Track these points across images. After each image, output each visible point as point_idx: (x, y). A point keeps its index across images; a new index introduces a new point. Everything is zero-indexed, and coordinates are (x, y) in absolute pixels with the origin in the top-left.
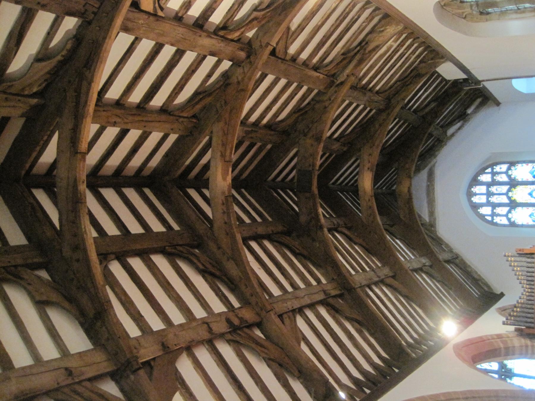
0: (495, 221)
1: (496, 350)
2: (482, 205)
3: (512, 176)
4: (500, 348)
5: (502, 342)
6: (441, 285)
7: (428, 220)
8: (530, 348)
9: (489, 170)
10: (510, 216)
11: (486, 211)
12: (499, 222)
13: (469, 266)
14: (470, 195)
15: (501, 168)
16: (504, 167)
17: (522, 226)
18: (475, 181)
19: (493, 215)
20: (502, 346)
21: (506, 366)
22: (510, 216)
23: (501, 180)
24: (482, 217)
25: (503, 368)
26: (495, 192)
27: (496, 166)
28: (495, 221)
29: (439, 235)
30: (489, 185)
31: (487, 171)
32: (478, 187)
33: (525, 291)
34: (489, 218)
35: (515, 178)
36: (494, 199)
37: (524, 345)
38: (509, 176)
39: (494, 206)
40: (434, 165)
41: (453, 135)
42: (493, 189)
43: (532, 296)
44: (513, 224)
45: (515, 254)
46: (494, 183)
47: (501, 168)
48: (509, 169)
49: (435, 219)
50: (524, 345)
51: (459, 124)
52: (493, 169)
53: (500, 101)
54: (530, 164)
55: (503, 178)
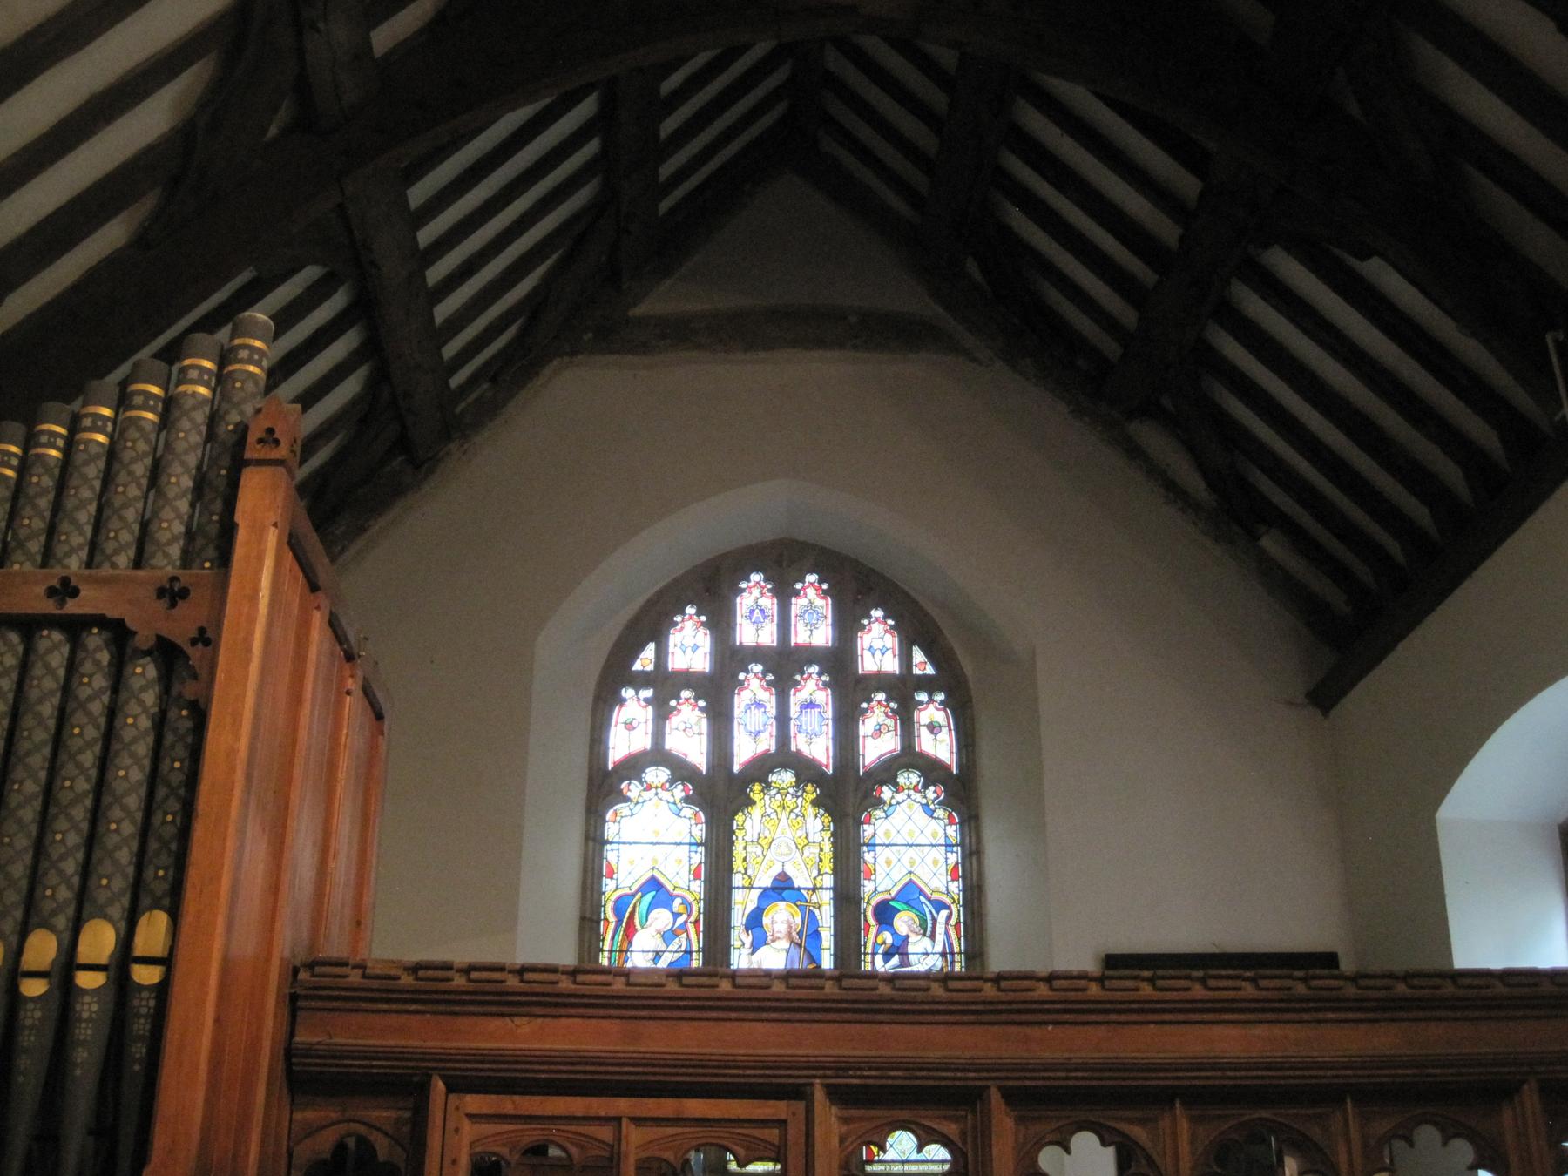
0: (627, 693)
2: (720, 622)
3: (886, 793)
7: (638, 311)
9: (922, 665)
10: (657, 775)
11: (689, 644)
12: (621, 715)
13: (362, 530)
14: (779, 563)
15: (933, 728)
16: (940, 746)
17: (594, 841)
18: (858, 588)
19: (665, 686)
22: (657, 775)
23: (866, 728)
24: (652, 624)
26: (796, 699)
27: (945, 704)
28: (627, 693)
29: (547, 371)
30: (838, 663)
31: (918, 656)
32: (824, 606)
34: (645, 660)
35: (879, 803)
36: (753, 697)
38: (887, 772)
39: (716, 693)
41: (1134, 451)
42: (813, 688)
44: (604, 787)
46: (851, 690)
47: (933, 728)
48: (931, 770)
49: (643, 348)
51: (1195, 483)
52: (927, 684)
53: (1333, 712)
54: (956, 887)
55: (877, 740)
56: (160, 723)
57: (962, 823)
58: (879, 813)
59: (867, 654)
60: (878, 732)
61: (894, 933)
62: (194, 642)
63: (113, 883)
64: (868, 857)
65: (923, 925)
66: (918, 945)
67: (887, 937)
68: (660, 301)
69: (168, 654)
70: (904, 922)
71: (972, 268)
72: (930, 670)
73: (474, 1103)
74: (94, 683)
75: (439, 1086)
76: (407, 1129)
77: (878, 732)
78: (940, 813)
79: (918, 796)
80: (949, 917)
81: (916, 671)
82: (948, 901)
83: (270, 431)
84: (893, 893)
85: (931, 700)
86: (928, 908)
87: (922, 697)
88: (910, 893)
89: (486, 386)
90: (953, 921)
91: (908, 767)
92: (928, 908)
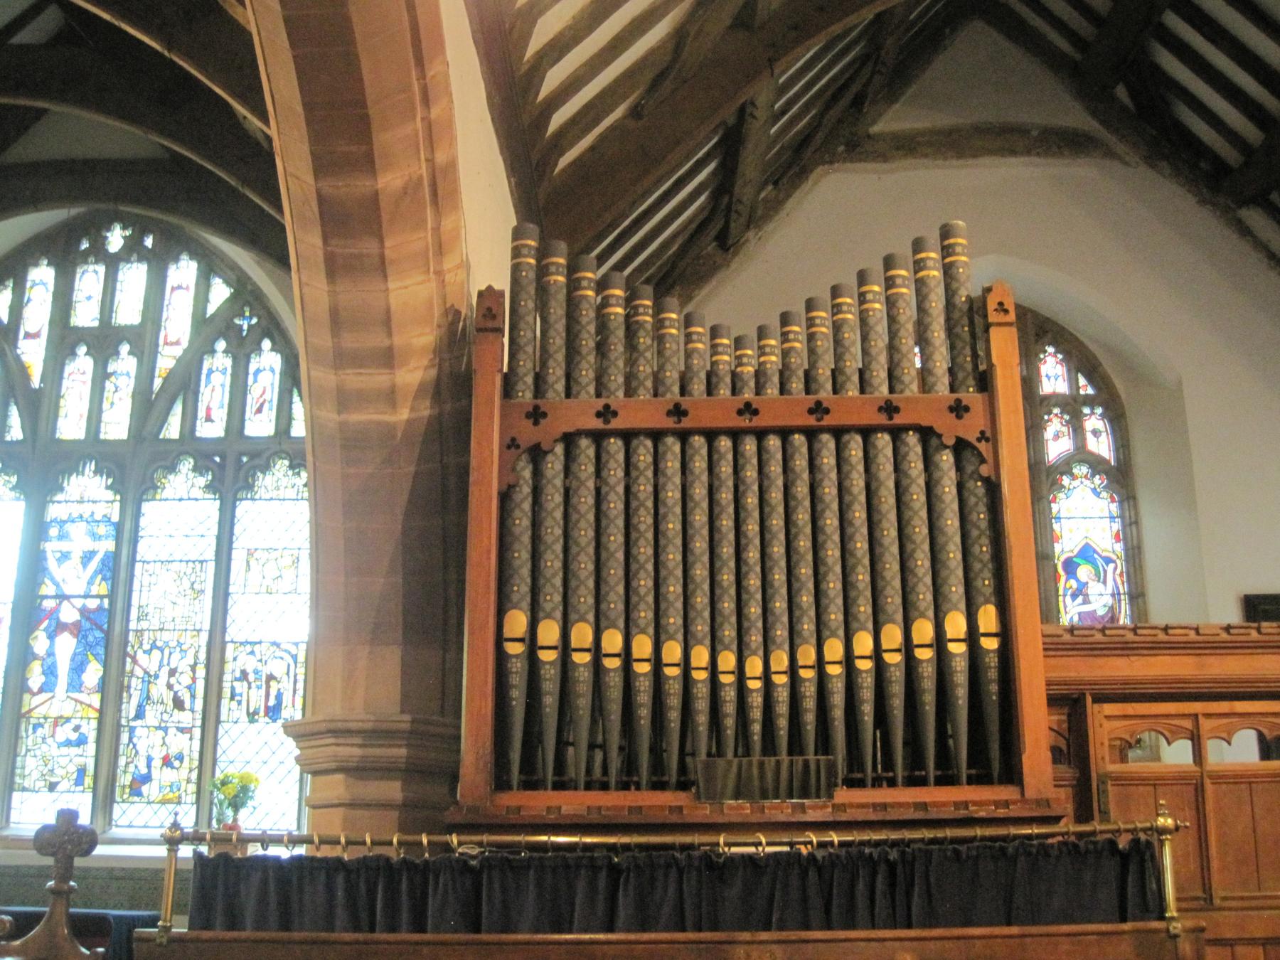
1: (361, 127)
3: (1066, 480)
4: (367, 163)
5: (410, 190)
6: (652, 52)
7: (875, 129)
8: (377, 379)
15: (1096, 433)
16: (1102, 446)
20: (389, 181)
21: (266, 468)
23: (1049, 433)
25: (253, 456)
27: (1103, 416)
29: (813, 176)
31: (1082, 381)
33: (739, 343)
37: (398, 340)
38: (1065, 466)
40: (1110, 154)
41: (1245, 231)
43: (710, 391)
45: (968, 289)
47: (1096, 433)
48: (1097, 465)
50: (398, 340)
52: (1090, 401)
54: (1119, 547)
56: (960, 487)
57: (1121, 502)
58: (1061, 495)
59: (1044, 379)
60: (1057, 437)
61: (1078, 580)
62: (979, 440)
63: (956, 590)
64: (1056, 526)
65: (1097, 575)
66: (1094, 588)
67: (1073, 583)
68: (892, 120)
69: (960, 447)
70: (1084, 572)
71: (1121, 92)
72: (1090, 391)
73: (1109, 709)
74: (915, 466)
75: (1089, 699)
76: (1065, 726)
77: (1057, 437)
78: (1104, 494)
79: (1087, 482)
80: (1115, 569)
81: (1082, 392)
82: (1114, 557)
83: (1001, 304)
84: (1076, 552)
85: (1093, 413)
86: (1100, 562)
87: (1086, 410)
88: (1087, 553)
89: (770, 187)
90: (1118, 571)
91: (1081, 461)
92: (1100, 562)
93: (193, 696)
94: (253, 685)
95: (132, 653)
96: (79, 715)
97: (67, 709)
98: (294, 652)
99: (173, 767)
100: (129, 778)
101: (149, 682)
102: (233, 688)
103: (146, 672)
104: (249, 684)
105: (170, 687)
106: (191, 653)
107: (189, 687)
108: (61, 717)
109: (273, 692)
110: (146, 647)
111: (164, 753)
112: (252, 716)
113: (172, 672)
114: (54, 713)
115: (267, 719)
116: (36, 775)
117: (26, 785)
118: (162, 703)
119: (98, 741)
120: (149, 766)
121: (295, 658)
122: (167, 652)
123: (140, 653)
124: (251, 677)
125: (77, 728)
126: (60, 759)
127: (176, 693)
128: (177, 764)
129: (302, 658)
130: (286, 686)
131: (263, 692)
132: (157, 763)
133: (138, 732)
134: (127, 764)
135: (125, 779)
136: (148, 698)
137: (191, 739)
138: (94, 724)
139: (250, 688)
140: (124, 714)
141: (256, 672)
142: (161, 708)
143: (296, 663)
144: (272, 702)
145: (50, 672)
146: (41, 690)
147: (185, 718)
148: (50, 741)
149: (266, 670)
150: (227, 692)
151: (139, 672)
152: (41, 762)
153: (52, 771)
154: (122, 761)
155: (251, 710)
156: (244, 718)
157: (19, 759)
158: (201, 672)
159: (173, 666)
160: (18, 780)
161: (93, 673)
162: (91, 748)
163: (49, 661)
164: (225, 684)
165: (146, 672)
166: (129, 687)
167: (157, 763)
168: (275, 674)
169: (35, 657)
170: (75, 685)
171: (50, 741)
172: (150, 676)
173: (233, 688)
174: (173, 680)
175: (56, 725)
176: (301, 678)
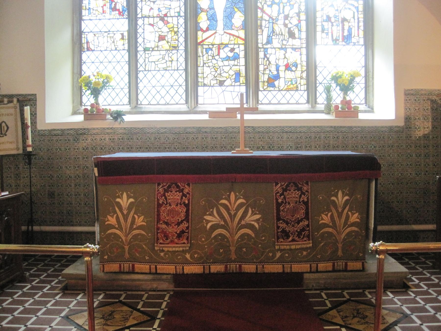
93: (300, 31)
94: (334, 24)
95: (261, 6)
96: (232, 42)
97: (226, 39)
98: (356, 5)
99: (292, 71)
100: (266, 77)
101: (273, 23)
102: (323, 26)
103: (270, 17)
104: (332, 23)
105: (285, 25)
106: (296, 6)
107: (297, 26)
108: (222, 44)
109: (346, 28)
110: (269, 3)
111: (285, 63)
112: (335, 41)
113: (286, 17)
114: (217, 42)
115: (344, 43)
116: (211, 77)
117: (206, 82)
118: (282, 34)
119: (246, 57)
120: (278, 70)
121: (357, 8)
122: (281, 5)
123: (265, 6)
124: (333, 20)
125: (232, 50)
126: (224, 68)
127: (289, 29)
128: (294, 68)
129: (361, 8)
130: (354, 24)
131: (340, 28)
132: (282, 68)
133: (269, 51)
134: (265, 69)
135: (263, 78)
136: (273, 31)
137: (301, 55)
138: (242, 47)
139: (332, 25)
140: (259, 41)
141: (335, 17)
142: (281, 38)
143: (358, 11)
144: (346, 33)
145: (212, 18)
146: (208, 29)
147: (296, 43)
148: (217, 58)
149: (341, 16)
150: (319, 29)
151: (266, 17)
152: (213, 70)
153: (220, 74)
154: (261, 68)
155: (334, 38)
156: (331, 42)
157: (199, 68)
158: (303, 17)
159: (286, 13)
160: (200, 80)
161: (238, 18)
162: (242, 61)
163: (211, 12)
164: (317, 24)
165: (270, 17)
166: (261, 26)
167: (282, 68)
168: (348, 18)
169: (202, 10)
170: (228, 24)
171: (217, 58)
172: (273, 19)
173: (323, 26)
174: (287, 22)
175: (219, 49)
176: (361, 20)
